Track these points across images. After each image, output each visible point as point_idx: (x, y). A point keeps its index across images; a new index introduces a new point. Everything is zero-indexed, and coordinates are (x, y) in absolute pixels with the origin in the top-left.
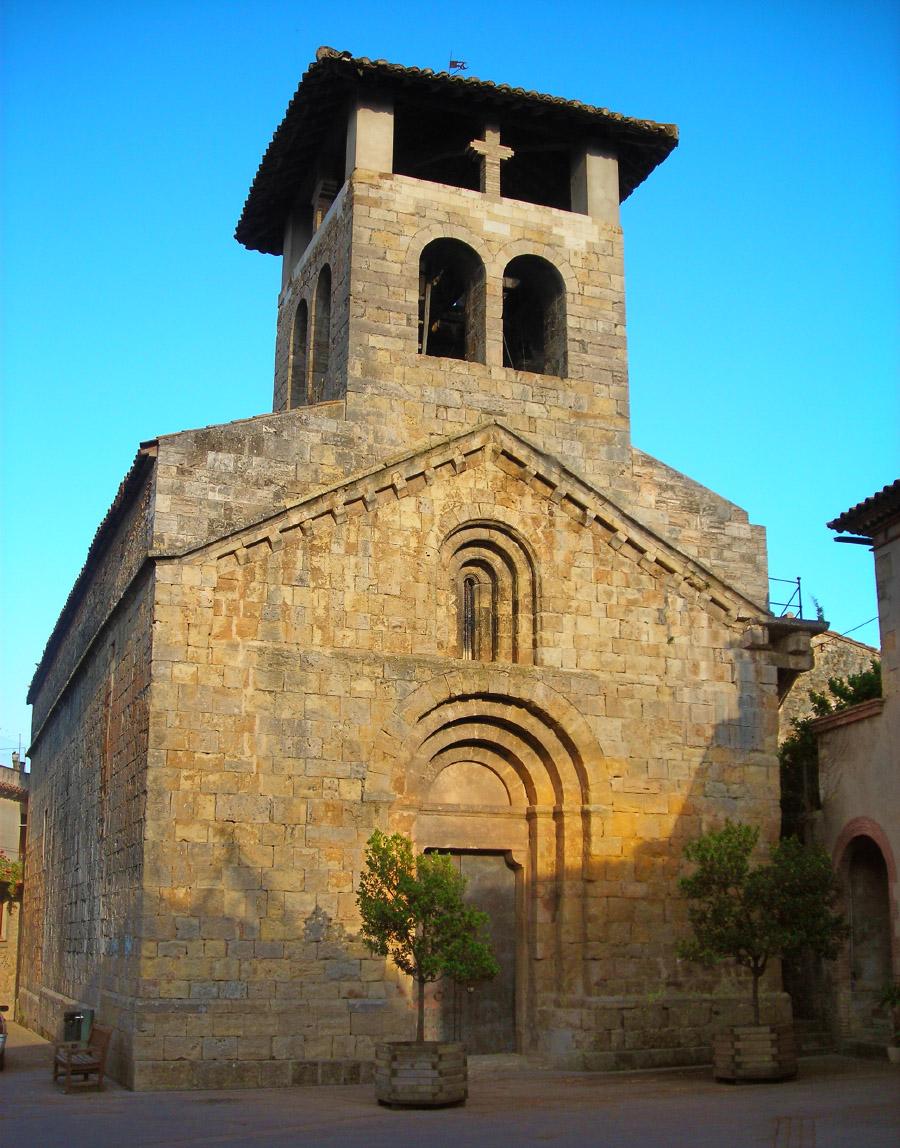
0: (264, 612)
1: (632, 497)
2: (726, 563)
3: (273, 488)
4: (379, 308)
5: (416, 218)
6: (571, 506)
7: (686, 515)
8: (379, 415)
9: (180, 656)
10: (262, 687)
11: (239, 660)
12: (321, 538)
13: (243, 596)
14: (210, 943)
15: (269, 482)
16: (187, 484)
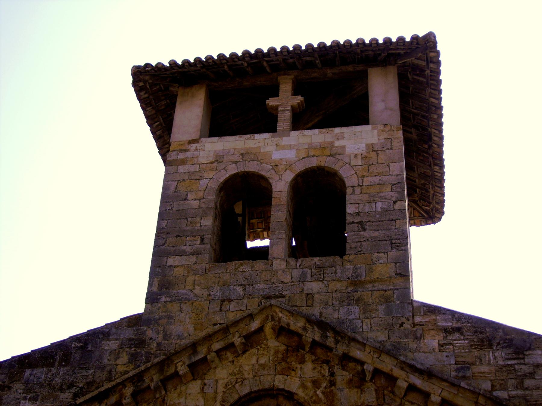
1: (413, 345)
2: (527, 392)
3: (74, 390)
5: (215, 164)
6: (351, 365)
7: (476, 353)
8: (170, 317)
15: (71, 385)
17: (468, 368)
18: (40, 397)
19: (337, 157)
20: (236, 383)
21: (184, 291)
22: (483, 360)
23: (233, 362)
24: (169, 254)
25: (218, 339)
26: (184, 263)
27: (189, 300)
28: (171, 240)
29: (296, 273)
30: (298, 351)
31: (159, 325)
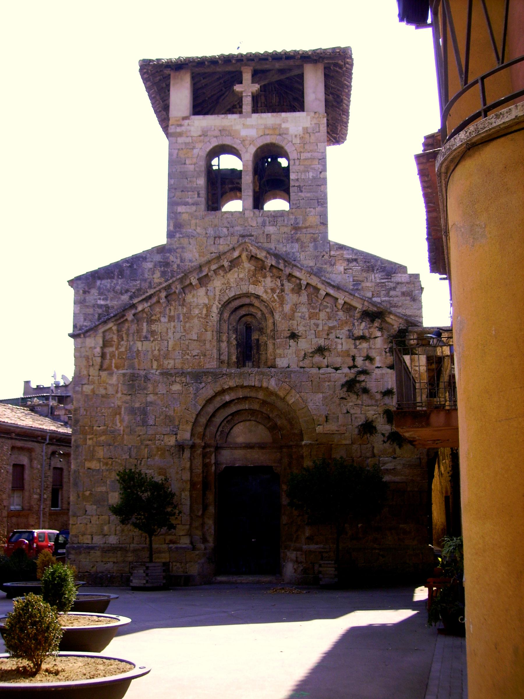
0: (128, 355)
1: (329, 269)
2: (391, 299)
3: (129, 294)
4: (182, 191)
5: (202, 138)
7: (365, 274)
8: (183, 248)
9: (85, 381)
10: (125, 392)
11: (114, 380)
12: (156, 315)
13: (117, 349)
14: (101, 517)
15: (127, 291)
16: (87, 298)
17: (360, 284)
18: (109, 298)
19: (284, 136)
20: (226, 289)
21: (190, 230)
22: (368, 279)
23: (223, 276)
24: (178, 204)
26: (188, 211)
27: (194, 237)
28: (178, 193)
29: (260, 220)
30: (262, 270)
31: (177, 252)
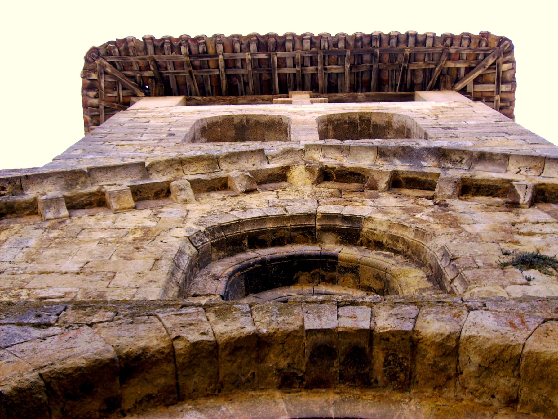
25: (197, 172)
